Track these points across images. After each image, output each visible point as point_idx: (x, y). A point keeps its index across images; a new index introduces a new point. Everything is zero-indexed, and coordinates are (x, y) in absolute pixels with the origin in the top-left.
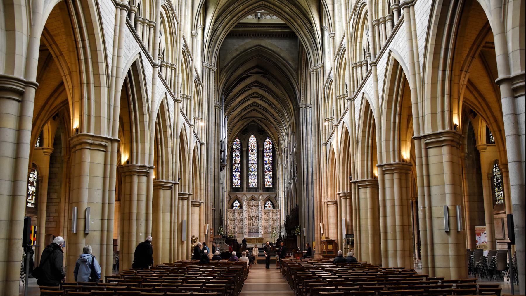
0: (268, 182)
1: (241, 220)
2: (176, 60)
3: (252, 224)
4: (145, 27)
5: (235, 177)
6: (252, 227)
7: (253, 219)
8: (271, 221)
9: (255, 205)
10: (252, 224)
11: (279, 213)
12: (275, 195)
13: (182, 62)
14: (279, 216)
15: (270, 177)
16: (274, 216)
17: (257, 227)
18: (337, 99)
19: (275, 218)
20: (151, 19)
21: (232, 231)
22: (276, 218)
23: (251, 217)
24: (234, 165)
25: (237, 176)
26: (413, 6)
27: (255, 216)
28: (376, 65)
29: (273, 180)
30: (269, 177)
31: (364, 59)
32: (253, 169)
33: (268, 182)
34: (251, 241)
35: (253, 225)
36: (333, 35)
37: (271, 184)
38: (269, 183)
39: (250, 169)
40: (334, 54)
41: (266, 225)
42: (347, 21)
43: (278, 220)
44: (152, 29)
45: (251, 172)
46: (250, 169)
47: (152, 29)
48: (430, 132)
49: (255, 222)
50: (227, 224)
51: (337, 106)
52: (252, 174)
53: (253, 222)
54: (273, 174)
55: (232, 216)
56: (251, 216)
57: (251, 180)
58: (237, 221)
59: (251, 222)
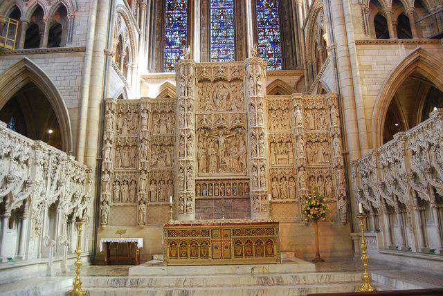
0: (270, 56)
1: (165, 145)
3: (213, 160)
5: (170, 44)
6: (215, 176)
7: (222, 140)
8: (300, 146)
9: (229, 76)
10: (213, 160)
11: (334, 111)
12: (298, 78)
14: (335, 120)
15: (274, 43)
16: (312, 126)
17: (241, 175)
19: (317, 131)
21: (125, 195)
22: (321, 131)
23: (208, 129)
24: (168, 14)
25: (178, 41)
27: (229, 124)
29: (282, 50)
30: (271, 42)
32: (222, 24)
33: (270, 56)
34: (205, 243)
35: (220, 165)
37: (279, 61)
38: (272, 59)
39: (216, 24)
41: (282, 164)
43: (337, 140)
45: (219, 30)
46: (216, 24)
49: (227, 153)
50: (100, 161)
52: (220, 34)
53: (221, 153)
54: (281, 36)
55: (125, 129)
56: (211, 123)
57: (219, 51)
58: (146, 148)
59: (211, 151)
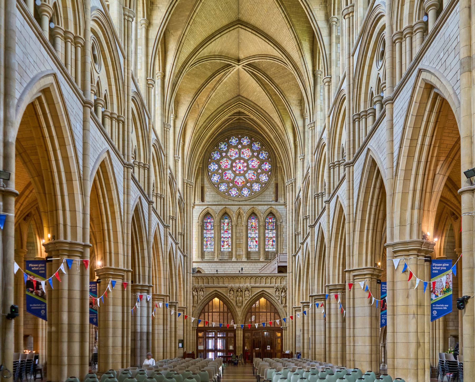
2: (164, 190)
4: (141, 169)
13: (153, 154)
18: (304, 219)
20: (145, 162)
26: (353, 166)
28: (329, 203)
31: (343, 158)
36: (303, 158)
40: (303, 176)
42: (312, 154)
44: (146, 171)
47: (146, 171)
48: (316, 294)
51: (329, 177)
